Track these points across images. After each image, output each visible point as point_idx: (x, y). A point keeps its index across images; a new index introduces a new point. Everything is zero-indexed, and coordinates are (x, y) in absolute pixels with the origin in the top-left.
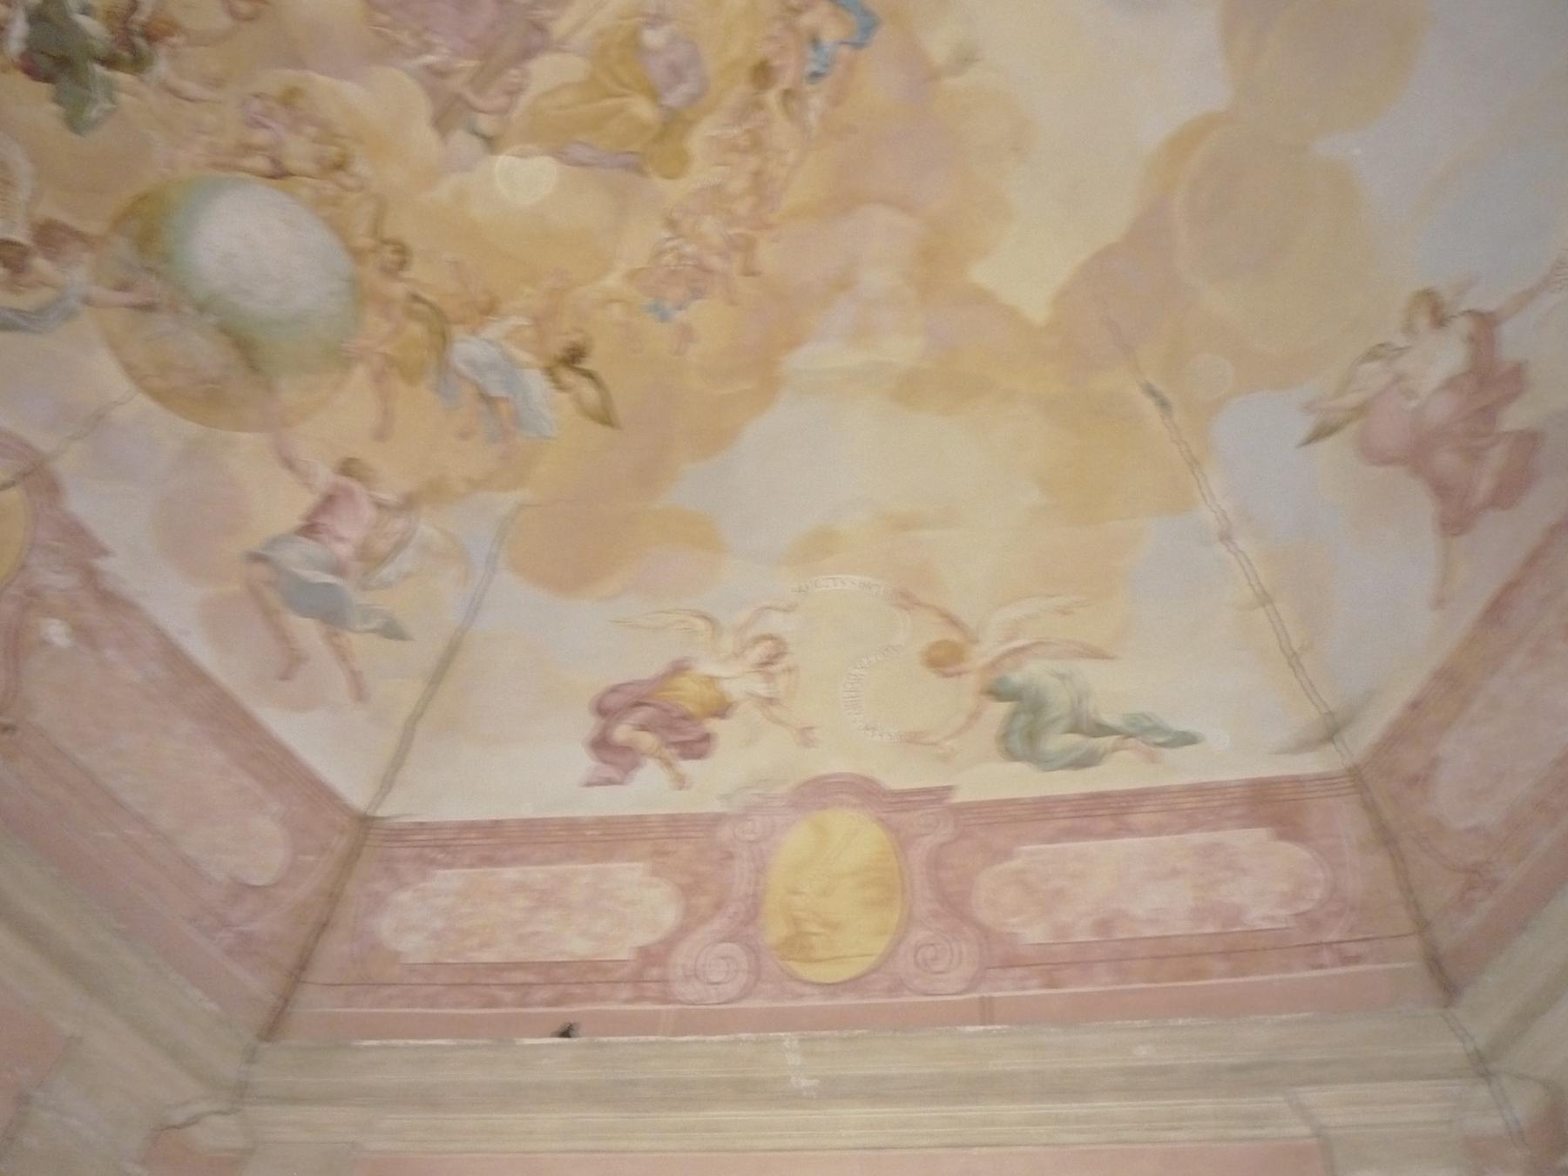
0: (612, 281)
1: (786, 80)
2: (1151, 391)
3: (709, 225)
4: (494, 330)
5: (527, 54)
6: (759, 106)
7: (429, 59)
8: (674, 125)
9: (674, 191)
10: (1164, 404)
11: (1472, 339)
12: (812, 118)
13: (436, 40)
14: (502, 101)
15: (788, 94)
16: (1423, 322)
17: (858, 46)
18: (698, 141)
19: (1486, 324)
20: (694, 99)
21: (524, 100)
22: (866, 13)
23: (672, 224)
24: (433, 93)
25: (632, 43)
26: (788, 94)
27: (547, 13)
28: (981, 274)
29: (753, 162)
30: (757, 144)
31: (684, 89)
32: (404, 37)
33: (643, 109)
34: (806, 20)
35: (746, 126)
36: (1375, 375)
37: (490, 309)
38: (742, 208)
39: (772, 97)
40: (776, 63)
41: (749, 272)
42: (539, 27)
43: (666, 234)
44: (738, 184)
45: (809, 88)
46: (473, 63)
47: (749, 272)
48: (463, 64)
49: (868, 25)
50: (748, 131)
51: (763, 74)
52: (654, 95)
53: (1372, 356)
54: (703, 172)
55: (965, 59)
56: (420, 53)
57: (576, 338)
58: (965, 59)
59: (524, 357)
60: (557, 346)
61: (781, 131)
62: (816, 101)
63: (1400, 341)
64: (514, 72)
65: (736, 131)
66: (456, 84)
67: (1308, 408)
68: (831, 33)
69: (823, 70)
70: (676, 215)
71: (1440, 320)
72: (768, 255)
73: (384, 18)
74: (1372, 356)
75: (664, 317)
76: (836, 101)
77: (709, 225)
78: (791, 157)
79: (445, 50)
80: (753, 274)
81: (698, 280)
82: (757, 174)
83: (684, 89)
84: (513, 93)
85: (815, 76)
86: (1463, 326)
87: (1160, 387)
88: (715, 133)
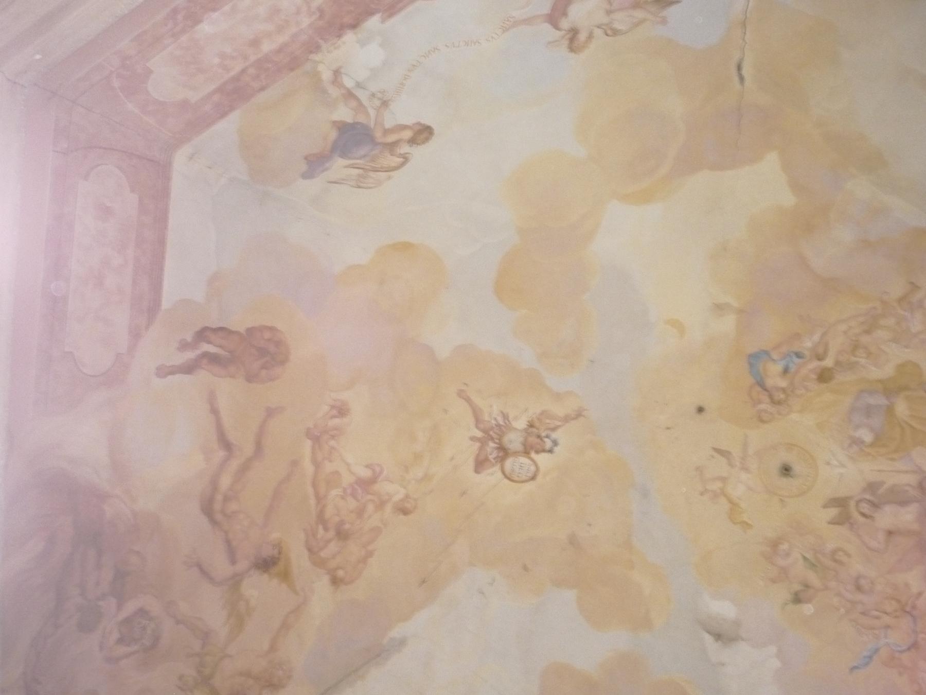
1: (815, 364)
2: (742, 79)
6: (838, 363)
8: (890, 389)
10: (739, 68)
11: (565, 14)
12: (816, 338)
15: (820, 358)
16: (582, 37)
17: (766, 353)
18: (887, 371)
19: (553, 19)
22: (751, 365)
25: (879, 440)
26: (820, 358)
28: (788, 199)
29: (865, 339)
30: (856, 346)
33: (901, 408)
34: (783, 383)
35: (853, 359)
36: (621, 21)
38: (891, 322)
39: (829, 362)
40: (814, 376)
44: (880, 334)
45: (807, 353)
49: (755, 359)
51: (824, 376)
52: (890, 410)
53: (616, 32)
54: (896, 355)
55: (719, 308)
58: (719, 308)
61: (837, 343)
62: (808, 344)
63: (598, 32)
65: (863, 361)
67: (664, 21)
68: (775, 369)
71: (574, 33)
72: (897, 289)
74: (616, 32)
76: (797, 336)
78: (843, 327)
80: (912, 283)
82: (868, 332)
83: (872, 401)
85: (799, 355)
86: (565, 24)
87: (736, 79)
88: (873, 368)
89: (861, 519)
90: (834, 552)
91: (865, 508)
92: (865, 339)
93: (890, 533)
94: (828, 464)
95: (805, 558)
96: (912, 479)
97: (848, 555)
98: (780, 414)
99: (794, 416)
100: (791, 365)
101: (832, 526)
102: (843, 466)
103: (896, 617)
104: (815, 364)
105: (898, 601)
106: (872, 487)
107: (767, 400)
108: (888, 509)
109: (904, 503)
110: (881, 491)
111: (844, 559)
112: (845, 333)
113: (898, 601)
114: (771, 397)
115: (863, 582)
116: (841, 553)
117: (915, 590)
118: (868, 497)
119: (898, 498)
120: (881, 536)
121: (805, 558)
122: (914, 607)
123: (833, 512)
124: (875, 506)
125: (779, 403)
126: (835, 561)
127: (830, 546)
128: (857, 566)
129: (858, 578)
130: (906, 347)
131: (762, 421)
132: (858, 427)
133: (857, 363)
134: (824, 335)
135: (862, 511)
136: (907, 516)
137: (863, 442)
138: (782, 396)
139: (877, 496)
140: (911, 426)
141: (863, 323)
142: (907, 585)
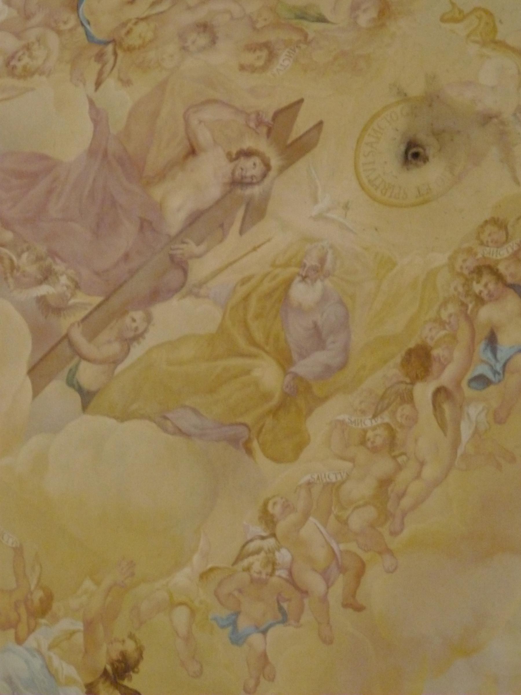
0: (183, 578)
1: (446, 378)
3: (312, 530)
4: (42, 636)
5: (156, 295)
6: (408, 398)
7: (44, 290)
9: (277, 478)
12: (466, 431)
13: (59, 267)
14: (115, 348)
15: (440, 392)
18: (319, 424)
20: (329, 371)
21: (137, 351)
23: (268, 519)
24: (38, 333)
27: (191, 247)
29: (383, 466)
30: (392, 442)
31: (321, 357)
32: (25, 262)
33: (268, 375)
34: (486, 314)
35: (385, 418)
37: (44, 609)
38: (357, 521)
39: (424, 392)
40: (435, 352)
41: (353, 604)
42: (181, 265)
43: (259, 530)
44: (361, 489)
45: (468, 392)
46: (97, 300)
47: (353, 604)
48: (80, 298)
50: (388, 426)
51: (419, 361)
52: (285, 361)
56: (40, 283)
57: (130, 646)
59: (67, 670)
60: (102, 661)
61: (426, 436)
62: (476, 412)
64: (138, 315)
65: (368, 423)
66: (65, 323)
69: (490, 375)
70: (275, 510)
72: (376, 585)
73: (8, 236)
75: (237, 639)
76: (499, 418)
77: (312, 530)
78: (429, 472)
79: (64, 280)
80: (359, 609)
81: (289, 599)
82: (385, 483)
83: (321, 357)
84: (129, 341)
85: (482, 381)
88: (345, 417)
89: (248, 144)
90: (272, 56)
91: (251, 167)
92: (383, 466)
93: (193, 152)
94: (346, 207)
95: (321, 19)
96: (199, 270)
97: (242, 68)
98: (470, 251)
99: (440, 259)
100: (489, 355)
101: (294, 99)
102: (320, 217)
103: (124, 25)
104: (446, 378)
105: (130, 49)
106: (256, 211)
107: (502, 268)
108: (215, 192)
109: (195, 218)
110: (240, 213)
111: (249, 58)
112: (422, 464)
113: (130, 49)
114: (499, 277)
115: (203, 40)
116: (260, 63)
117: (111, 83)
118: (256, 191)
119: (206, 222)
120: (204, 136)
121: (321, 19)
122: (100, 57)
123: (302, 124)
124: (237, 182)
125: (478, 271)
126: (266, 45)
127: (283, 61)
128: (223, 57)
129: (214, 41)
130: (309, 484)
131: (494, 221)
132: (324, 298)
133: (375, 416)
134: (456, 443)
135: (257, 160)
136: (178, 201)
137: (304, 278)
138: (477, 288)
139: (242, 201)
140: (242, 355)
141: (401, 496)
142: (126, 83)
